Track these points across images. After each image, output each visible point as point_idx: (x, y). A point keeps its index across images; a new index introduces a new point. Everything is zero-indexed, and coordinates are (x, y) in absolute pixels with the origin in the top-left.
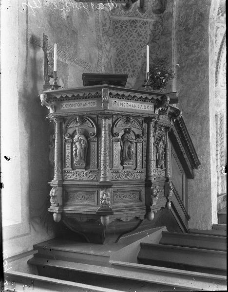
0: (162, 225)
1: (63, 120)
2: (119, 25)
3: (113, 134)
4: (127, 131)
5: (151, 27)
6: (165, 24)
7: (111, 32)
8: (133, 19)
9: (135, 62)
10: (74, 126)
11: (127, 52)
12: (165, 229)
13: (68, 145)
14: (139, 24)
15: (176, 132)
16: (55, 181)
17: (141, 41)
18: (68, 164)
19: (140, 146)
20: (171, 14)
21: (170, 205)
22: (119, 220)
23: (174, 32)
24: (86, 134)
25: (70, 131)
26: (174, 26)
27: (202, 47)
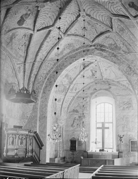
1: (8, 134)
3: (19, 138)
4: (22, 137)
5: (33, 106)
6: (36, 106)
7: (21, 107)
10: (11, 136)
12: (32, 162)
13: (9, 140)
15: (36, 137)
19: (25, 141)
21: (33, 156)
23: (39, 108)
24: (13, 138)
27: (46, 113)
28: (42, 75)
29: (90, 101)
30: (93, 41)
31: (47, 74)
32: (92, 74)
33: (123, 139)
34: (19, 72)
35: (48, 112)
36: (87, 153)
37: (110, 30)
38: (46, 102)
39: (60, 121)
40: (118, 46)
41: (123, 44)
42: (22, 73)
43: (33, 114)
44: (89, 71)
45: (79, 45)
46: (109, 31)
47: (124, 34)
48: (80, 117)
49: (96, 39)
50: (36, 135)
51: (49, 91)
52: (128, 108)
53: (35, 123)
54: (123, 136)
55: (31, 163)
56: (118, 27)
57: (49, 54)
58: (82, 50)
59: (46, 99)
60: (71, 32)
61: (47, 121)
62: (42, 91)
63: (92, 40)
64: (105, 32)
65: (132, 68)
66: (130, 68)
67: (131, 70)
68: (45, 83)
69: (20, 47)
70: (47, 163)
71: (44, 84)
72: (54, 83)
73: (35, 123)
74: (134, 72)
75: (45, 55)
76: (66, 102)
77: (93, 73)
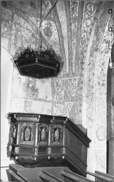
2: (65, 81)
8: (70, 78)
11: (68, 92)
14: (72, 80)
17: (73, 87)
28: (86, 29)
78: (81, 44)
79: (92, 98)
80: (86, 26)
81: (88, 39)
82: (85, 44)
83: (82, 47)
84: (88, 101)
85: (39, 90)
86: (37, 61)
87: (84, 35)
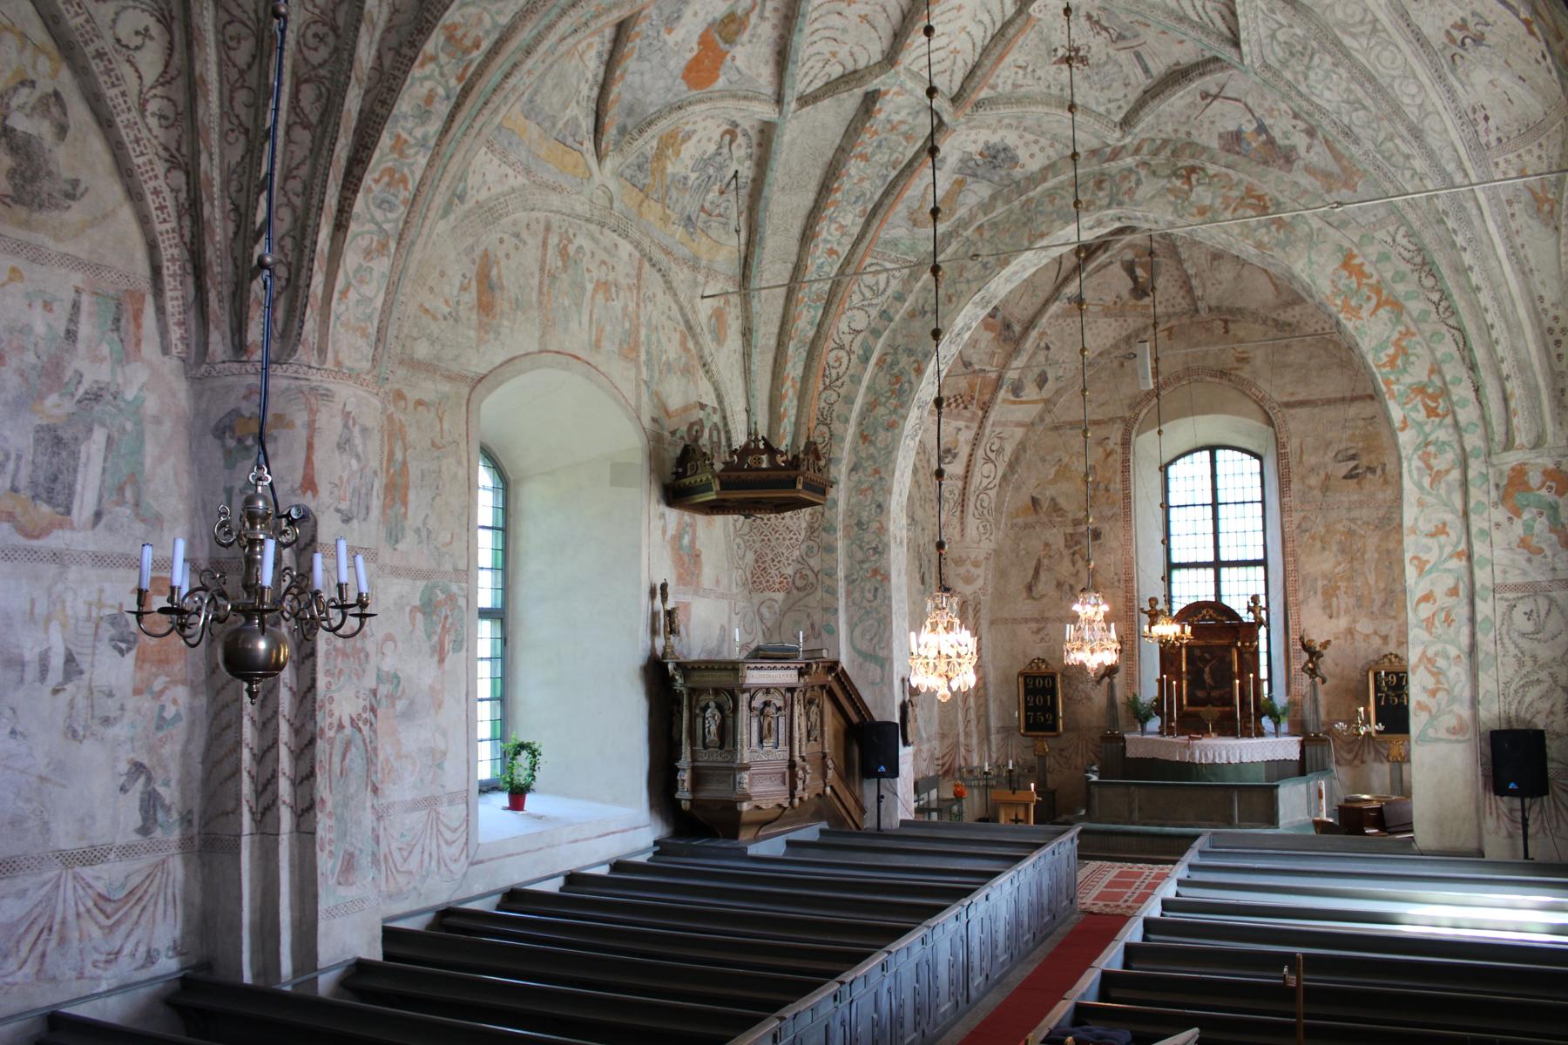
0: (817, 816)
1: (694, 692)
3: (751, 709)
4: (766, 704)
9: (784, 571)
12: (824, 825)
13: (699, 721)
16: (685, 762)
18: (699, 742)
20: (835, 503)
21: (828, 790)
22: (758, 807)
23: (840, 526)
24: (719, 707)
25: (703, 704)
26: (840, 518)
27: (881, 554)
28: (847, 339)
29: (1126, 443)
30: (1126, 123)
31: (876, 333)
32: (1130, 284)
33: (1327, 664)
34: (719, 339)
35: (893, 545)
36: (1124, 748)
37: (1227, 53)
38: (877, 488)
39: (962, 570)
40: (1280, 141)
41: (1311, 132)
42: (734, 341)
43: (812, 562)
44: (1116, 268)
45: (1042, 149)
46: (1216, 59)
47: (1312, 75)
48: (1072, 541)
49: (1147, 110)
50: (837, 678)
51: (891, 426)
52: (1357, 476)
53: (825, 610)
54: (1326, 644)
55: (822, 832)
56: (1273, 36)
57: (875, 223)
58: (1062, 178)
59: (877, 471)
60: (993, 87)
61: (890, 598)
62: (851, 430)
63: (1118, 118)
64: (1197, 65)
65: (1368, 269)
66: (1359, 272)
67: (1359, 284)
68: (865, 383)
69: (710, 196)
70: (904, 823)
71: (862, 390)
72: (913, 378)
73: (825, 610)
74: (1379, 292)
75: (856, 231)
76: (988, 460)
77: (1135, 279)
78: (821, 387)
79: (876, 589)
80: (847, 330)
81: (856, 380)
82: (842, 391)
83: (823, 396)
84: (857, 595)
85: (704, 558)
86: (800, 487)
87: (838, 359)
